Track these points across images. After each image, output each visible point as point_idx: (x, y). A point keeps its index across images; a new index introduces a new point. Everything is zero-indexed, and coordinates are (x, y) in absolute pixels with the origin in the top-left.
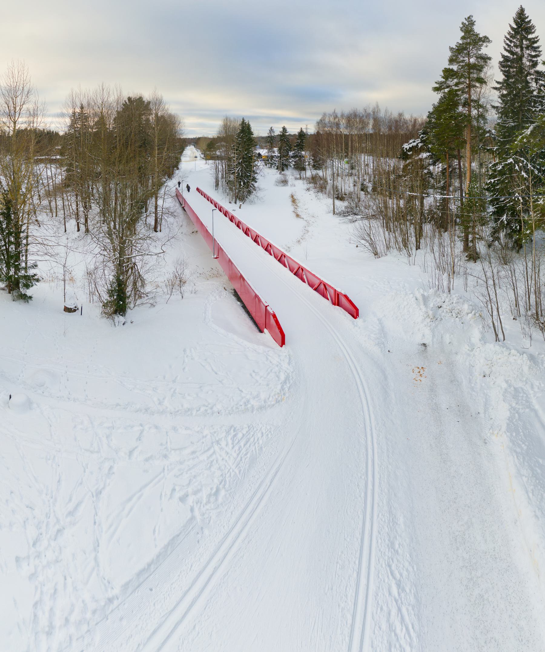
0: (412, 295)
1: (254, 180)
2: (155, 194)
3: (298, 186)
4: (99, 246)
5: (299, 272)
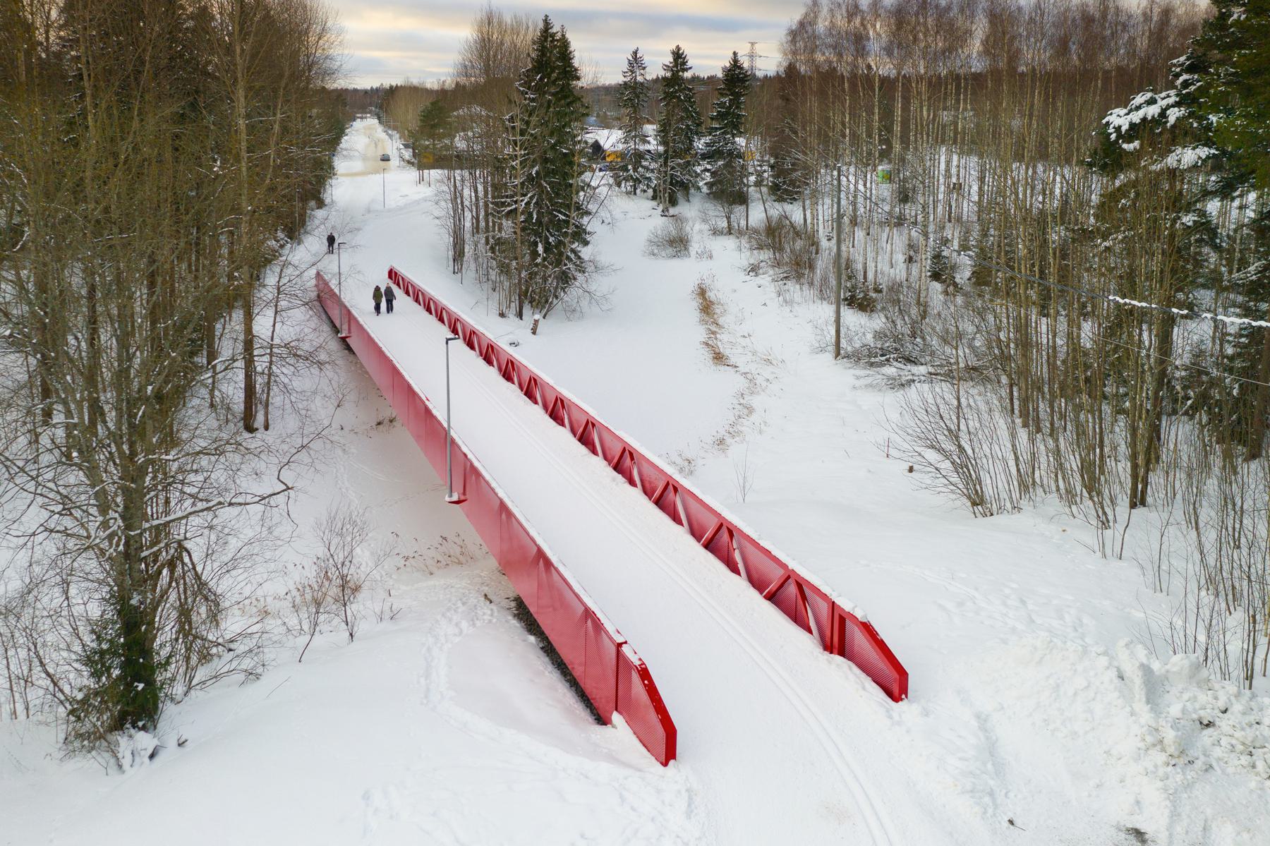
0: (1104, 661)
1: (580, 235)
2: (243, 299)
3: (723, 260)
4: (40, 500)
5: (719, 540)
